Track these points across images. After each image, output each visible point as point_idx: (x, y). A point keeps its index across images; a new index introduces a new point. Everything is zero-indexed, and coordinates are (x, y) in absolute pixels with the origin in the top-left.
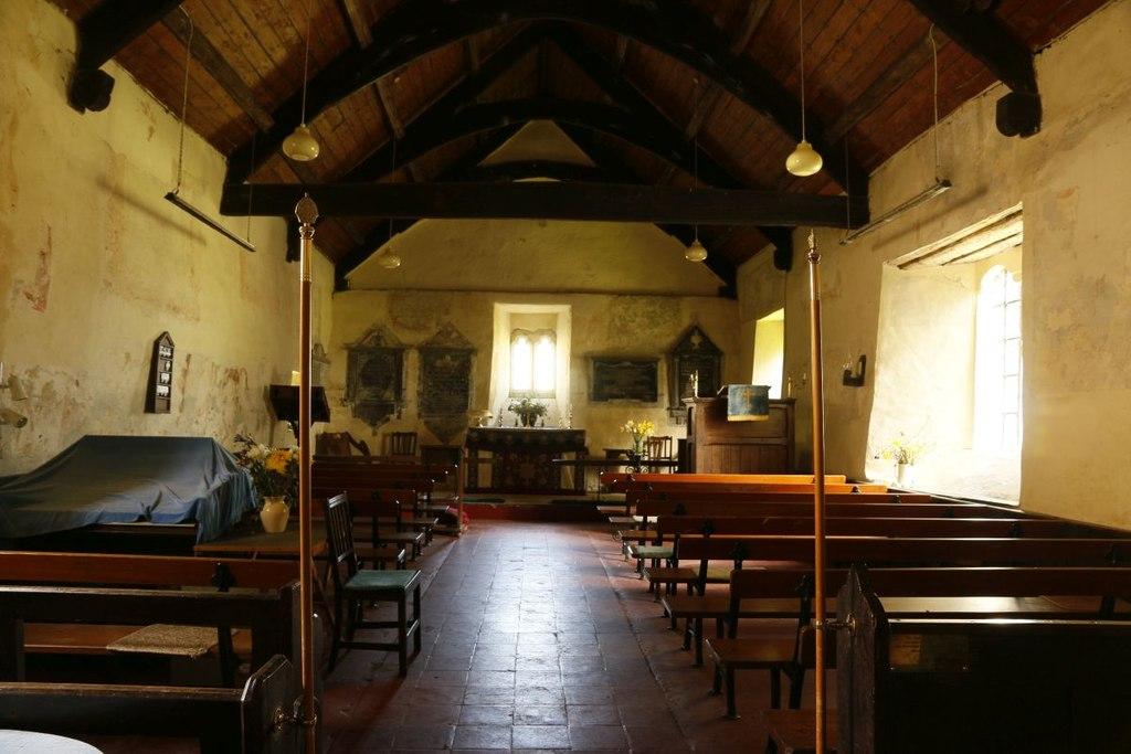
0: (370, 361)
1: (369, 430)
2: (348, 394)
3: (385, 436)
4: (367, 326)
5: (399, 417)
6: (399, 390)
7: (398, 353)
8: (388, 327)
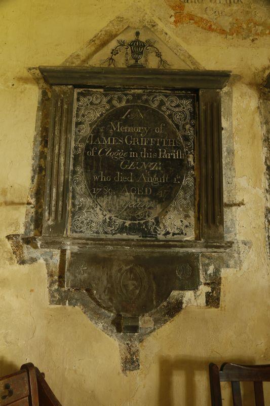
0: (115, 115)
1: (110, 347)
2: (37, 221)
3: (167, 368)
4: (98, 25)
5: (213, 300)
6: (211, 208)
7: (201, 91)
8: (161, 25)
